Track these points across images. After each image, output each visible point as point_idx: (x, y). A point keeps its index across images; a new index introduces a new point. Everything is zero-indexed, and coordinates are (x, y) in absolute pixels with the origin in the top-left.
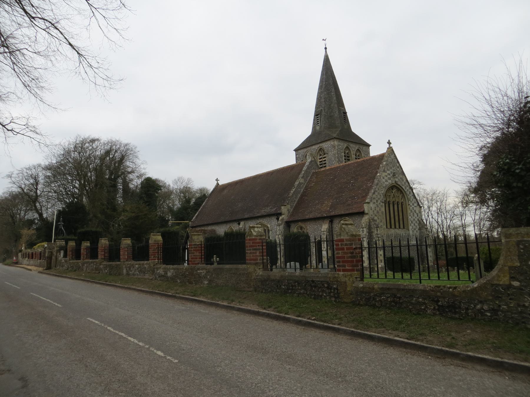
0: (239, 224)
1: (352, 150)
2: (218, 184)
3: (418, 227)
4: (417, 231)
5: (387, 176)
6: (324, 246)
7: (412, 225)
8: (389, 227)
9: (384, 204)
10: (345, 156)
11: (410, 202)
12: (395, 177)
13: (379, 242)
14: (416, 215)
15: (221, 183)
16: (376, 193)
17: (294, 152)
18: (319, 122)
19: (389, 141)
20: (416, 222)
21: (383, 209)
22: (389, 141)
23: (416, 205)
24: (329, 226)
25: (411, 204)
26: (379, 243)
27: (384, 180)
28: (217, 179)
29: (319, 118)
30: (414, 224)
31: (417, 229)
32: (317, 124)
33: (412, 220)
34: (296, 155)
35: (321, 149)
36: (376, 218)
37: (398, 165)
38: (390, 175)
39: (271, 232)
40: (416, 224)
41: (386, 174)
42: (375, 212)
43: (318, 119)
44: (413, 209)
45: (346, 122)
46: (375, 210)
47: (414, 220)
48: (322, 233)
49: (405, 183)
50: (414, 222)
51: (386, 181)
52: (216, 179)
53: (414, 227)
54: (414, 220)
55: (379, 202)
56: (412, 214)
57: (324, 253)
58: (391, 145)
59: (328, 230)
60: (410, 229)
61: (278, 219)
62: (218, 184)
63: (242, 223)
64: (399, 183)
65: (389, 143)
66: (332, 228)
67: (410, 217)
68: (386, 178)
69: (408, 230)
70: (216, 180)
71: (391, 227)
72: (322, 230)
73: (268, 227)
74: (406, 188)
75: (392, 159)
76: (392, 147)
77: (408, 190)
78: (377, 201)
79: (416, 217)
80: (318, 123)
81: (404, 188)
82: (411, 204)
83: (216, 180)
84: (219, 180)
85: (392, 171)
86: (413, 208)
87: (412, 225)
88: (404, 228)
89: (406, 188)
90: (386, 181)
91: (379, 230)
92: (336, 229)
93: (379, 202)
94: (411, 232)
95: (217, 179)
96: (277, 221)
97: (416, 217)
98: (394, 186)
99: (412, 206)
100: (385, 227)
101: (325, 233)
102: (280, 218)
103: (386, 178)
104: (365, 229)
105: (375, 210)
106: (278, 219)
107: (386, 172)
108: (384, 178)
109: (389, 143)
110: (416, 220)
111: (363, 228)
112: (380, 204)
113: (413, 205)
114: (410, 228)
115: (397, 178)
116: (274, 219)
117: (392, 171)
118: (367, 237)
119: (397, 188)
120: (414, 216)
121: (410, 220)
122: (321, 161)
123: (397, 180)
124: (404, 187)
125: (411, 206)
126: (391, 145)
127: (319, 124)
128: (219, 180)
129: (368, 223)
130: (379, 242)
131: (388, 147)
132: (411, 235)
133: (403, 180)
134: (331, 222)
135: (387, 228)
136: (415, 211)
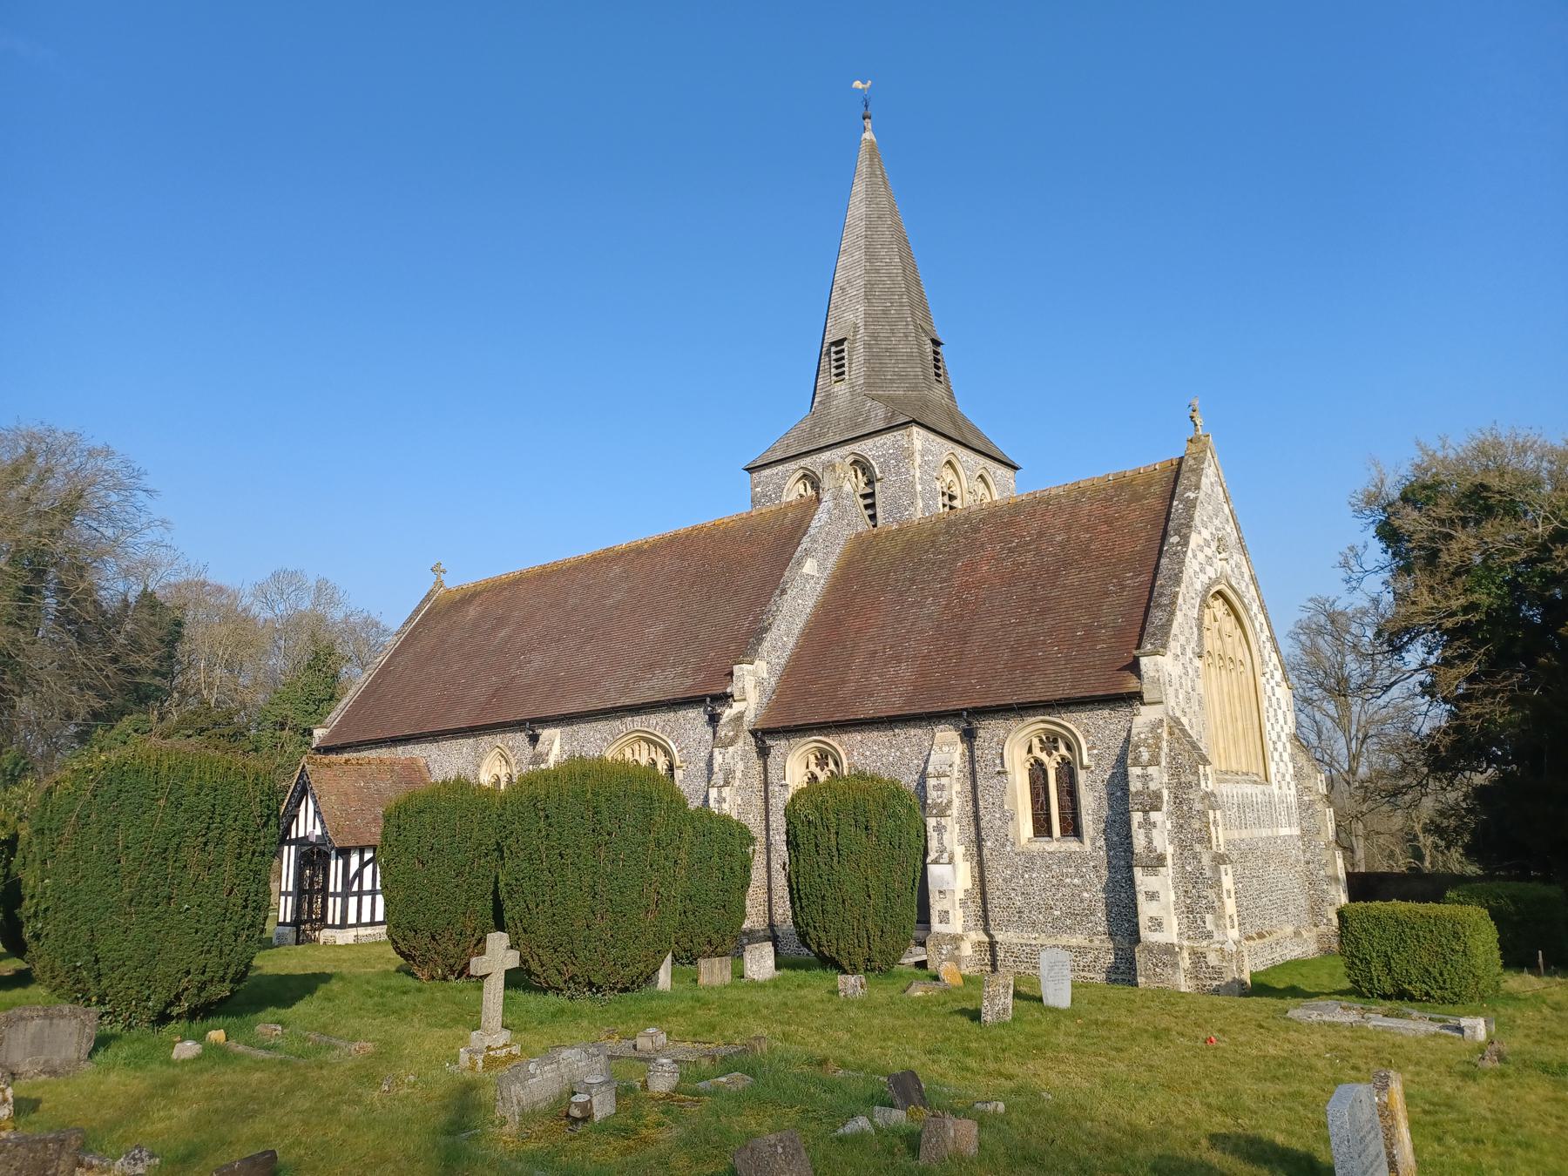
10: (943, 494)
36: (1184, 720)
40: (1286, 757)
55: (1189, 654)
61: (714, 719)
102: (728, 713)
106: (714, 719)
111: (1145, 767)
116: (696, 716)
127: (846, 376)
134: (969, 736)
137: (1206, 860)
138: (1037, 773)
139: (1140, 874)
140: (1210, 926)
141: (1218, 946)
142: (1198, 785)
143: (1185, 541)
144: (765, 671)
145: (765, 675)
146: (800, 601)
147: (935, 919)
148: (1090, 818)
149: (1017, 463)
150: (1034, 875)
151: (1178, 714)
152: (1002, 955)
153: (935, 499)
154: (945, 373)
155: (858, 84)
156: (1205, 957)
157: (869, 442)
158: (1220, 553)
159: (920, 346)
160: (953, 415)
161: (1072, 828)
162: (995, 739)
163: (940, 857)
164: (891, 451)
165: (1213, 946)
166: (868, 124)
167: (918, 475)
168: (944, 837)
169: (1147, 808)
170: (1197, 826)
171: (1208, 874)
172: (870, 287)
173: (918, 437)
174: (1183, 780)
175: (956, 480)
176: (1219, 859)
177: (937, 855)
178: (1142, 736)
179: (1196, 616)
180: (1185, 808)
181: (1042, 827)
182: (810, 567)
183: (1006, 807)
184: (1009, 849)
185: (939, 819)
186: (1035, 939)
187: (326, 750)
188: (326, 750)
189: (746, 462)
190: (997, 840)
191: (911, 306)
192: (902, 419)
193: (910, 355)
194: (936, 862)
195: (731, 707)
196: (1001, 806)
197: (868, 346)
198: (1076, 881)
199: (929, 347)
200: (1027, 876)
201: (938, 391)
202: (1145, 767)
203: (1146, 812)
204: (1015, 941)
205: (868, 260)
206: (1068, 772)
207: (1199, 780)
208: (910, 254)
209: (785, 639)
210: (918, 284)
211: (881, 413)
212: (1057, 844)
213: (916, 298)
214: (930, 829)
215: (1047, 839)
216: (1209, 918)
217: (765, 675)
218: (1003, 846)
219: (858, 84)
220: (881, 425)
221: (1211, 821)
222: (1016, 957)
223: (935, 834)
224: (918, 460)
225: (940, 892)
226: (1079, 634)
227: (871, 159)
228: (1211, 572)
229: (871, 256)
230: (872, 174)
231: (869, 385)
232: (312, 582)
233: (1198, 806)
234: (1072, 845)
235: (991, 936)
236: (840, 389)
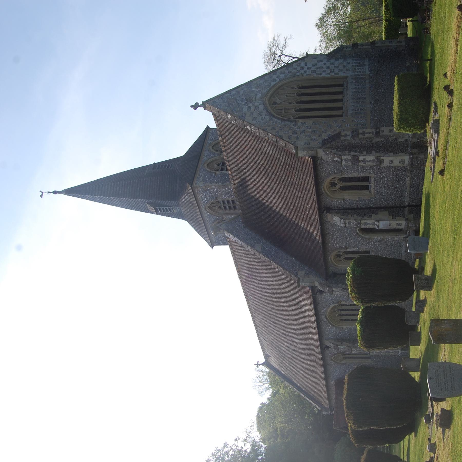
0: (328, 347)
1: (213, 157)
2: (263, 364)
3: (341, 61)
4: (348, 63)
5: (252, 113)
6: (369, 223)
7: (336, 71)
8: (339, 112)
9: (300, 120)
10: (222, 170)
11: (298, 74)
12: (254, 99)
13: (367, 133)
14: (320, 64)
15: (263, 360)
16: (281, 133)
17: (215, 247)
18: (168, 208)
19: (192, 106)
20: (333, 64)
21: (310, 121)
22: (192, 106)
23: (303, 64)
24: (337, 213)
25: (302, 71)
26: (370, 133)
28: (255, 364)
29: (161, 208)
30: (336, 67)
31: (345, 63)
32: (170, 211)
33: (328, 71)
34: (220, 244)
35: (209, 207)
36: (324, 136)
37: (233, 92)
38: (250, 107)
39: (343, 303)
40: (336, 63)
42: (314, 137)
43: (163, 209)
44: (311, 68)
45: (169, 166)
46: (309, 136)
47: (328, 67)
48: (347, 225)
49: (265, 81)
50: (332, 67)
51: (260, 114)
52: (255, 366)
53: (341, 67)
54: (328, 67)
55: (296, 128)
56: (318, 71)
57: (383, 225)
58: (200, 103)
59: (342, 216)
60: (345, 75)
62: (263, 364)
63: (327, 343)
65: (195, 107)
66: (339, 209)
67: (324, 75)
68: (255, 115)
69: (346, 78)
70: (258, 367)
71: (341, 108)
72: (343, 225)
73: (335, 307)
74: (274, 80)
76: (203, 102)
77: (278, 77)
78: (295, 132)
79: (325, 64)
80: (170, 209)
81: (274, 83)
82: (302, 71)
83: (258, 367)
84: (258, 362)
85: (244, 103)
86: (308, 69)
87: (336, 71)
88: (342, 85)
89: (274, 80)
90: (260, 114)
91: (346, 132)
92: (341, 202)
93: (296, 128)
94: (350, 74)
95: (255, 364)
96: (325, 294)
97: (325, 64)
98: (270, 98)
99: (306, 69)
100: (340, 119)
101: (347, 221)
102: (319, 288)
103: (255, 115)
104: (343, 157)
105: (309, 136)
106: (321, 292)
107: (245, 114)
109: (195, 107)
110: (328, 64)
111: (342, 160)
112: (299, 128)
113: (303, 68)
114: (341, 74)
115: (256, 95)
116: (320, 297)
117: (244, 103)
118: (357, 154)
119: (272, 95)
120: (322, 68)
121: (329, 74)
122: (230, 207)
123: (259, 95)
124: (273, 84)
125: (305, 72)
126: (200, 103)
127: (171, 208)
128: (258, 362)
129: (333, 151)
130: (367, 133)
131: (202, 108)
132: (354, 74)
135: (341, 116)
136: (314, 65)
137: (378, 139)
138: (344, 189)
139: (383, 165)
140: (403, 140)
141: (410, 138)
142: (349, 140)
144: (303, 272)
145: (304, 272)
146: (273, 253)
147: (400, 227)
148: (361, 174)
150: (384, 192)
151: (320, 140)
152: (414, 203)
156: (415, 143)
158: (253, 101)
161: (366, 179)
162: (331, 202)
163: (376, 225)
164: (205, 195)
165: (410, 140)
168: (368, 223)
169: (358, 161)
170: (365, 142)
171: (383, 139)
174: (347, 145)
176: (377, 134)
177: (375, 226)
178: (330, 158)
179: (280, 121)
180: (358, 145)
181: (366, 188)
183: (357, 200)
184: (373, 199)
185: (362, 224)
186: (407, 193)
190: (370, 203)
194: (378, 227)
195: (316, 287)
196: (357, 201)
198: (386, 179)
200: (384, 194)
202: (342, 160)
203: (360, 161)
204: (408, 199)
206: (343, 180)
207: (347, 140)
209: (289, 262)
212: (372, 186)
214: (366, 227)
215: (370, 187)
216: (400, 140)
217: (304, 272)
218: (372, 201)
221: (362, 137)
222: (414, 199)
223: (367, 226)
225: (390, 225)
226: (288, 168)
228: (261, 107)
233: (357, 141)
234: (372, 180)
235: (407, 206)
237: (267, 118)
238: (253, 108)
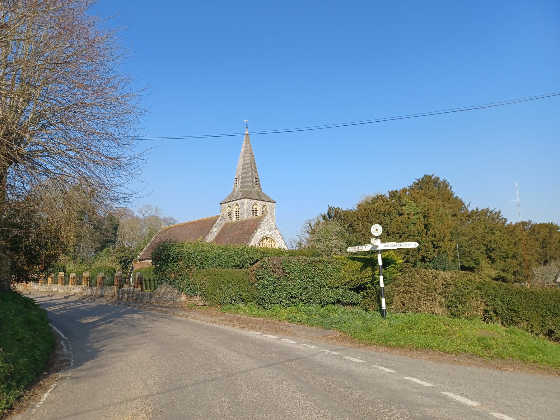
10: (253, 210)
27: (259, 234)
41: (262, 230)
64: (272, 235)
74: (278, 239)
75: (268, 220)
77: (280, 240)
90: (261, 234)
108: (259, 232)
122: (236, 214)
124: (276, 238)
133: (276, 234)
143: (256, 231)
149: (275, 201)
153: (250, 212)
154: (259, 183)
155: (245, 121)
157: (239, 201)
159: (252, 179)
160: (258, 193)
166: (247, 129)
167: (246, 208)
172: (243, 166)
173: (246, 201)
175: (257, 207)
182: (215, 230)
187: (140, 260)
188: (140, 260)
189: (220, 201)
191: (252, 170)
192: (243, 197)
193: (250, 181)
197: (242, 179)
199: (255, 179)
201: (257, 188)
205: (243, 161)
208: (254, 158)
210: (255, 164)
211: (241, 195)
213: (253, 168)
219: (245, 121)
220: (240, 198)
224: (246, 205)
227: (247, 138)
228: (265, 235)
229: (244, 160)
230: (246, 141)
231: (241, 188)
232: (154, 208)
236: (236, 188)
237: (260, 237)
238: (265, 231)
